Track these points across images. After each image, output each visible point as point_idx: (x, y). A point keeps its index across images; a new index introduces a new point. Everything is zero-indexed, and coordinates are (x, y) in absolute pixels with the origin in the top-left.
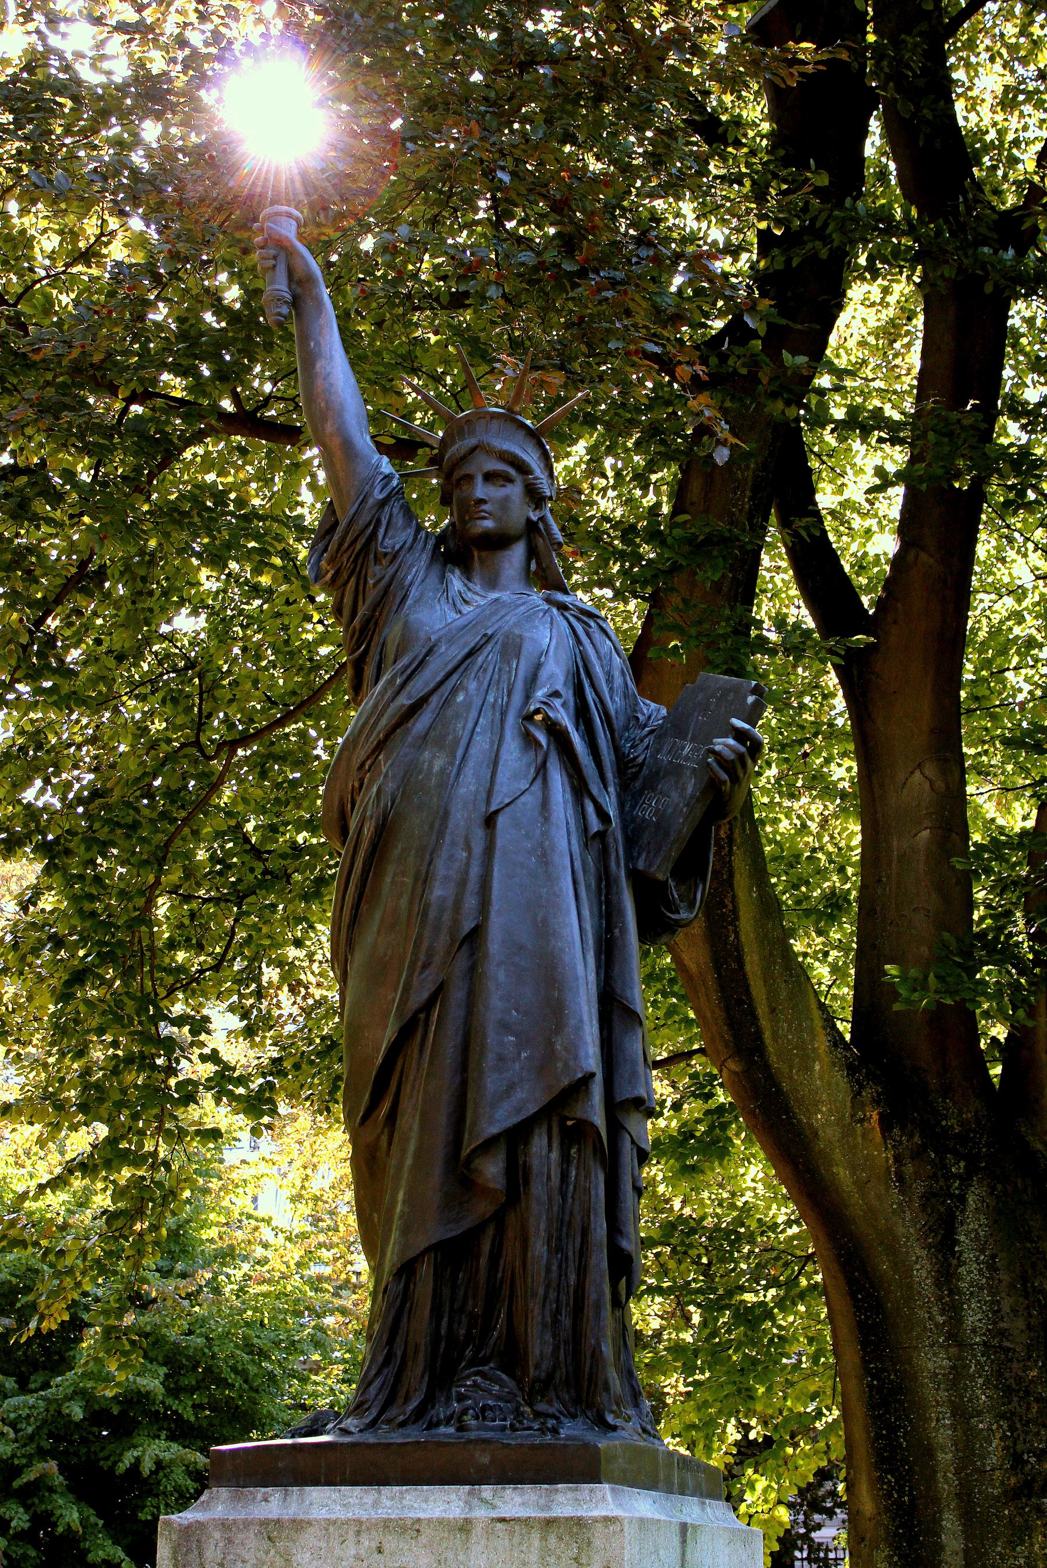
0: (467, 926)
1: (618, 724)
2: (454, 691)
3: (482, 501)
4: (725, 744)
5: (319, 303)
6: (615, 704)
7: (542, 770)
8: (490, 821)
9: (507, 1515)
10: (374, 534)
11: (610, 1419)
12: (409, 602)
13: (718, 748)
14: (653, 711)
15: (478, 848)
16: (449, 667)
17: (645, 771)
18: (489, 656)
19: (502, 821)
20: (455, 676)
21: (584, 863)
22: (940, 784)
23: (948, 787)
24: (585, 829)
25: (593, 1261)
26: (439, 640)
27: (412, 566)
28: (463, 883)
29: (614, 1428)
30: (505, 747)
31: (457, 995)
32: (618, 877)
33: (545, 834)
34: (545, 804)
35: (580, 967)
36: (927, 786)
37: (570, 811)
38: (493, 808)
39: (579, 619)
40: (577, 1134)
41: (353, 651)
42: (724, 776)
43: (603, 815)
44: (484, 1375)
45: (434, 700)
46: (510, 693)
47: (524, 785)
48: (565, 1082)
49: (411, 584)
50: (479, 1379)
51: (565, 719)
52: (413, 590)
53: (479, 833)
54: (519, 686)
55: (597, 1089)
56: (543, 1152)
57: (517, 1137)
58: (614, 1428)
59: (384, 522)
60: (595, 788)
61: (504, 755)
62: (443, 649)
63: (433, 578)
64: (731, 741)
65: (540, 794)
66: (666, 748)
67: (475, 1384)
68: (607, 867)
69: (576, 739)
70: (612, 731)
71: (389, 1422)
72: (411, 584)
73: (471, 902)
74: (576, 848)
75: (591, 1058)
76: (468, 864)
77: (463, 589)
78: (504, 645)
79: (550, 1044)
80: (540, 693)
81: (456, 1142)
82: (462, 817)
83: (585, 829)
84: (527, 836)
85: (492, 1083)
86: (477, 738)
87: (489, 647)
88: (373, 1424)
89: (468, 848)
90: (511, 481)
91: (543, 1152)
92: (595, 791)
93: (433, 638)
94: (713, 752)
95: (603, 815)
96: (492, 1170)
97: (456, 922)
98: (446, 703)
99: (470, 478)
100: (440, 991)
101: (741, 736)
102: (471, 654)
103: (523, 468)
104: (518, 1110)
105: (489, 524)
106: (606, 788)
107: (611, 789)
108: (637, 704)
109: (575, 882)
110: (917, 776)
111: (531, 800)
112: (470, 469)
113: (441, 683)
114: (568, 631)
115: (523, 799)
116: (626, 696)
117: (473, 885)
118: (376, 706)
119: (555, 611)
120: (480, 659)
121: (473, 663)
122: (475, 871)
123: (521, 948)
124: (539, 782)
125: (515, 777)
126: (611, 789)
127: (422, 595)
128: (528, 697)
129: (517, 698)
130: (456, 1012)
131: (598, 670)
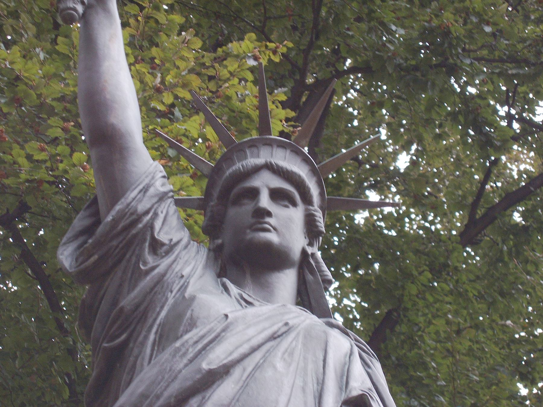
3: (269, 214)
20: (257, 356)
27: (186, 263)
49: (189, 276)
52: (192, 281)
62: (240, 327)
72: (189, 276)
87: (292, 335)
90: (294, 204)
99: (254, 193)
102: (274, 337)
105: (273, 237)
121: (274, 348)
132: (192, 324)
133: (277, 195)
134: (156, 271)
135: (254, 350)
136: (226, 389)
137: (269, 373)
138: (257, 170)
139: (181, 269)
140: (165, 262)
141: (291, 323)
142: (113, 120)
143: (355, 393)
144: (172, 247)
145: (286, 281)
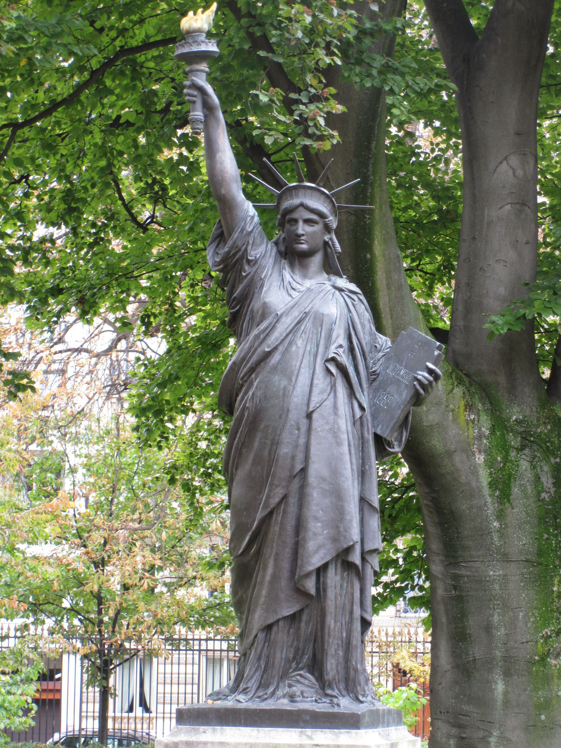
0: (299, 467)
1: (366, 350)
2: (290, 344)
3: (303, 235)
4: (423, 375)
5: (217, 120)
6: (365, 339)
7: (333, 387)
8: (309, 416)
9: (320, 743)
10: (246, 250)
11: (361, 698)
12: (265, 289)
13: (420, 377)
14: (384, 341)
15: (304, 429)
16: (288, 330)
17: (380, 378)
18: (308, 324)
19: (315, 416)
20: (291, 336)
21: (353, 434)
22: (520, 172)
23: (525, 174)
24: (354, 416)
25: (355, 626)
26: (282, 315)
28: (296, 446)
29: (362, 702)
30: (316, 376)
31: (293, 500)
32: (368, 440)
33: (335, 422)
34: (335, 407)
35: (351, 491)
36: (511, 173)
37: (347, 409)
38: (311, 409)
39: (349, 297)
40: (349, 566)
41: (233, 308)
42: (422, 391)
43: (362, 408)
44: (301, 675)
45: (281, 349)
46: (318, 347)
47: (325, 396)
48: (345, 546)
50: (298, 677)
51: (345, 359)
53: (305, 421)
54: (322, 342)
55: (358, 548)
56: (334, 577)
57: (321, 570)
58: (362, 702)
59: (251, 242)
60: (359, 394)
61: (315, 381)
62: (283, 319)
63: (275, 275)
64: (426, 375)
65: (332, 400)
66: (391, 367)
67: (298, 682)
68: (362, 434)
69: (351, 370)
70: (365, 359)
71: (259, 697)
73: (300, 456)
74: (350, 428)
75: (355, 534)
76: (298, 437)
77: (291, 280)
78: (315, 318)
79: (338, 527)
80: (333, 348)
81: (293, 572)
82: (296, 414)
83: (354, 416)
84: (327, 423)
85: (311, 545)
86: (302, 370)
88: (250, 699)
89: (298, 429)
91: (334, 577)
92: (358, 396)
93: (279, 313)
94: (417, 379)
95: (362, 408)
96: (310, 585)
97: (293, 467)
98: (287, 350)
99: (296, 221)
100: (285, 498)
101: (431, 372)
103: (322, 215)
104: (323, 558)
105: (304, 247)
106: (363, 391)
107: (366, 393)
108: (376, 339)
109: (349, 445)
110: (504, 167)
111: (329, 403)
112: (295, 215)
113: (283, 341)
114: (344, 304)
115: (325, 403)
116: (371, 334)
117: (301, 448)
118: (250, 348)
119: (337, 292)
120: (303, 327)
122: (302, 441)
123: (324, 480)
124: (332, 394)
125: (322, 392)
126: (366, 393)
127: (271, 285)
128: (327, 348)
129: (321, 349)
130: (292, 509)
131: (359, 327)
132: (263, 317)
133: (307, 221)
134: (249, 277)
135: (287, 335)
136: (276, 358)
137: (294, 348)
138: (297, 207)
139: (262, 272)
140: (254, 269)
141: (307, 310)
142: (223, 191)
143: (330, 357)
144: (256, 261)
145: (317, 260)
